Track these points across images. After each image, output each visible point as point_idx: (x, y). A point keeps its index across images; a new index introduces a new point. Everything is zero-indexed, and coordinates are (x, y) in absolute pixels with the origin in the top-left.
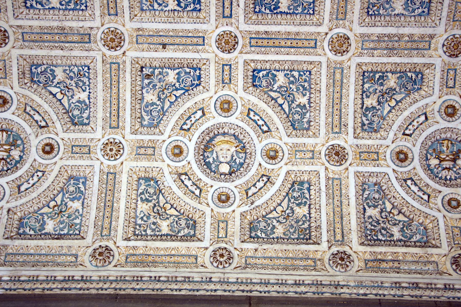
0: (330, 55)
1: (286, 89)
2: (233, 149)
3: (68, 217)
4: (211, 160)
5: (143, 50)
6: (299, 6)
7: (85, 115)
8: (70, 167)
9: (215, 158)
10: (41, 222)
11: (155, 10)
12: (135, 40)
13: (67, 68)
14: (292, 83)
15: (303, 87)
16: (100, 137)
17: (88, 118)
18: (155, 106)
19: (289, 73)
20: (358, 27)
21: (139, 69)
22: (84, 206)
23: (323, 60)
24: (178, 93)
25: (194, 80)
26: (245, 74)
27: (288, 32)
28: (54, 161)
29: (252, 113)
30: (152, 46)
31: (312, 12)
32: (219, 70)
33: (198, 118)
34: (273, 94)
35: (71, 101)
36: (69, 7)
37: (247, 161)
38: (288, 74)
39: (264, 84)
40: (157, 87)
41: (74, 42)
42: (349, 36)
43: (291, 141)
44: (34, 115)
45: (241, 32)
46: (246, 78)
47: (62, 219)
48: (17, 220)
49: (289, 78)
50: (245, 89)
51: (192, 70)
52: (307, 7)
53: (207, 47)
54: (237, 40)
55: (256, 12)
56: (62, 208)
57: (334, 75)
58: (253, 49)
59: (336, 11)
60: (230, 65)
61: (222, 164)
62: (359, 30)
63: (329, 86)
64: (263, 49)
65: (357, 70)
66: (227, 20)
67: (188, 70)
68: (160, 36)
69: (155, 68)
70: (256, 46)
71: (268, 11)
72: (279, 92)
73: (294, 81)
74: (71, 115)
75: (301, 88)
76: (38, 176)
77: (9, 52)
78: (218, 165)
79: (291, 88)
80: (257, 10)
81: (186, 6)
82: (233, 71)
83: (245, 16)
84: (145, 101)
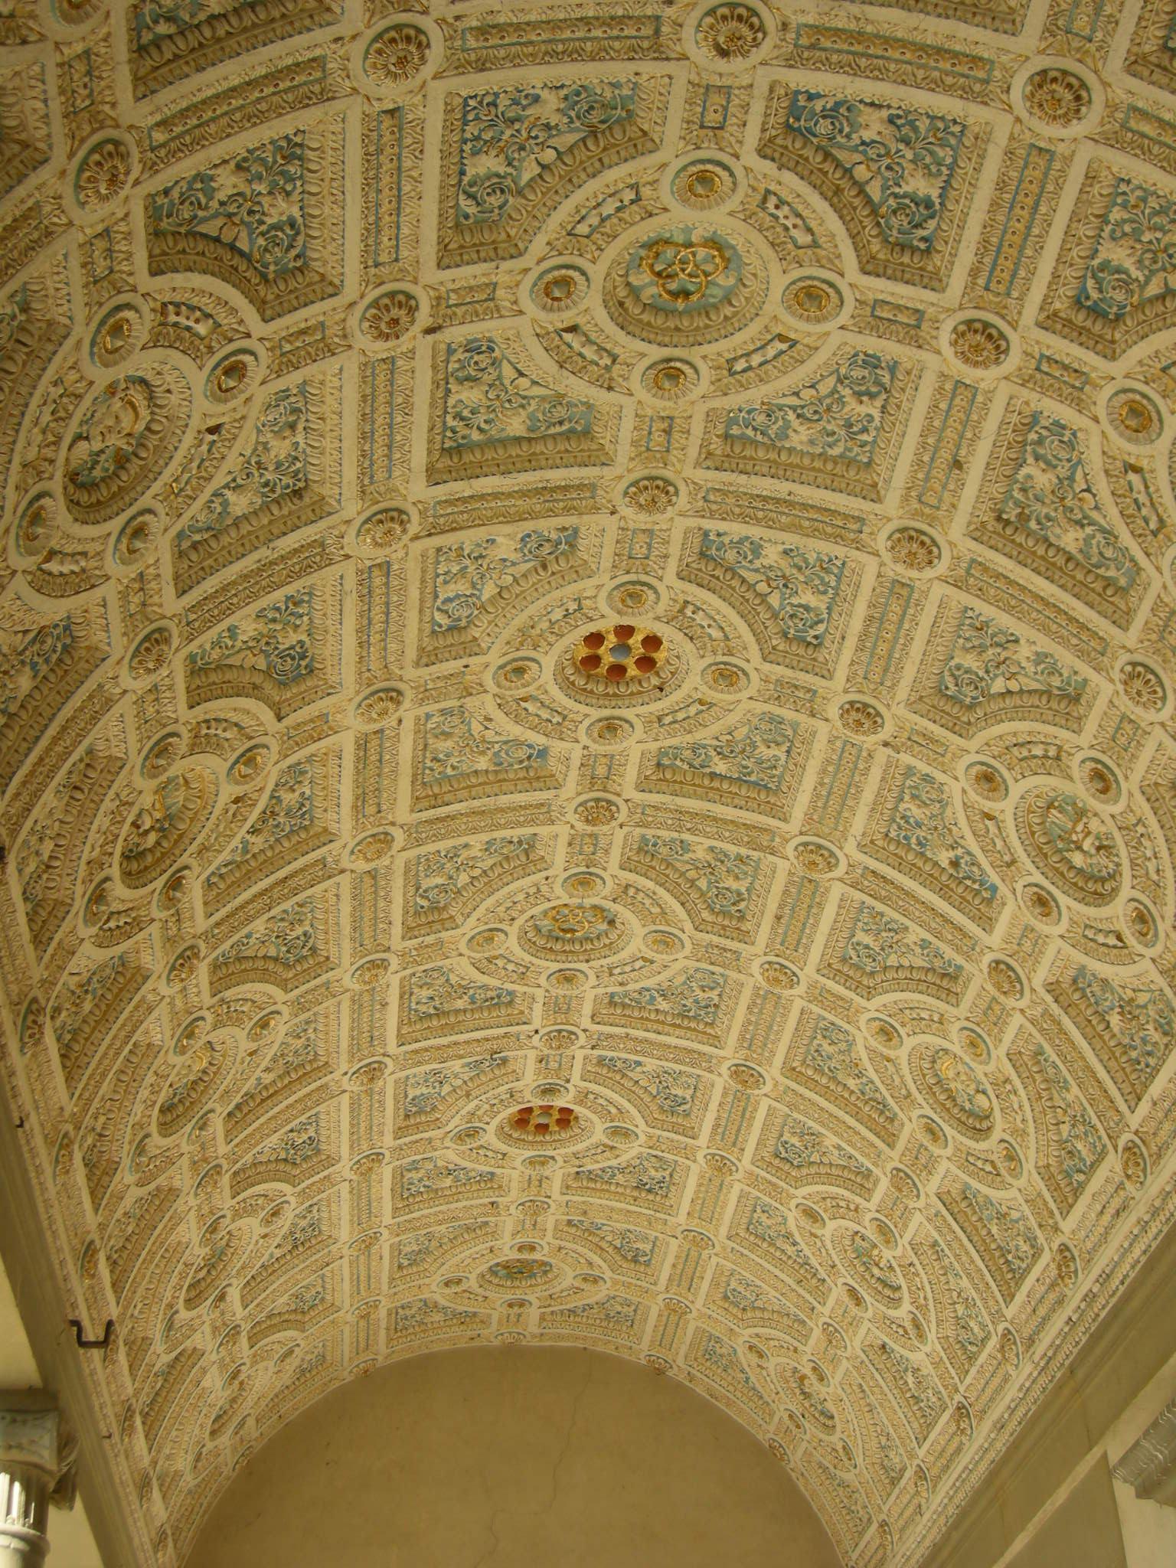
0: (1077, 129)
1: (1149, 255)
5: (954, 506)
6: (932, 153)
11: (875, 442)
12: (927, 511)
13: (961, 641)
14: (1136, 235)
15: (1156, 213)
16: (1111, 686)
18: (1094, 542)
19: (1110, 227)
20: (1019, 39)
21: (999, 527)
23: (1086, 153)
24: (1080, 484)
25: (1062, 435)
26: (1075, 334)
27: (992, 205)
28: (1124, 792)
30: (952, 487)
31: (957, 129)
32: (1047, 384)
33: (1142, 488)
34: (1154, 289)
36: (833, 584)
38: (1113, 231)
39: (1119, 296)
40: (1053, 514)
41: (904, 613)
42: (1039, 69)
45: (961, 308)
46: (1083, 339)
49: (1125, 234)
50: (1109, 352)
51: (1037, 428)
52: (940, 135)
53: (982, 385)
54: (978, 325)
55: (928, 248)
57: (1143, 135)
58: (1015, 294)
59: (962, 80)
60: (1042, 356)
62: (1029, 39)
63: (1165, 164)
64: (1022, 273)
65: (1146, 73)
66: (925, 326)
67: (1033, 436)
68: (932, 459)
69: (1009, 491)
70: (1011, 283)
71: (932, 224)
72: (1152, 273)
73: (1134, 225)
75: (1156, 219)
77: (894, 716)
79: (1150, 242)
80: (923, 246)
81: (878, 383)
82: (1057, 357)
83: (925, 287)
84: (1074, 552)
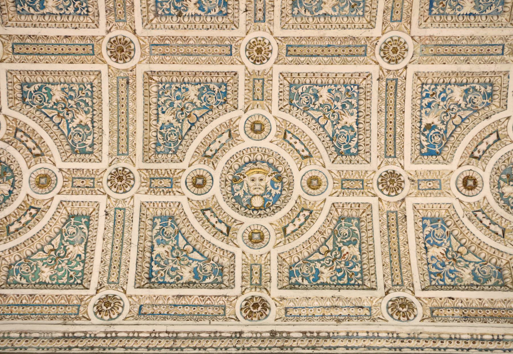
2: (268, 179)
3: (67, 264)
4: (241, 193)
7: (89, 142)
8: (70, 204)
9: (246, 191)
10: (35, 269)
17: (91, 146)
22: (87, 250)
29: (289, 136)
35: (70, 126)
37: (284, 192)
43: (336, 167)
44: (27, 141)
47: (60, 266)
48: (6, 267)
56: (60, 254)
61: (256, 197)
74: (71, 142)
76: (31, 213)
78: (250, 200)
79: (335, 106)
